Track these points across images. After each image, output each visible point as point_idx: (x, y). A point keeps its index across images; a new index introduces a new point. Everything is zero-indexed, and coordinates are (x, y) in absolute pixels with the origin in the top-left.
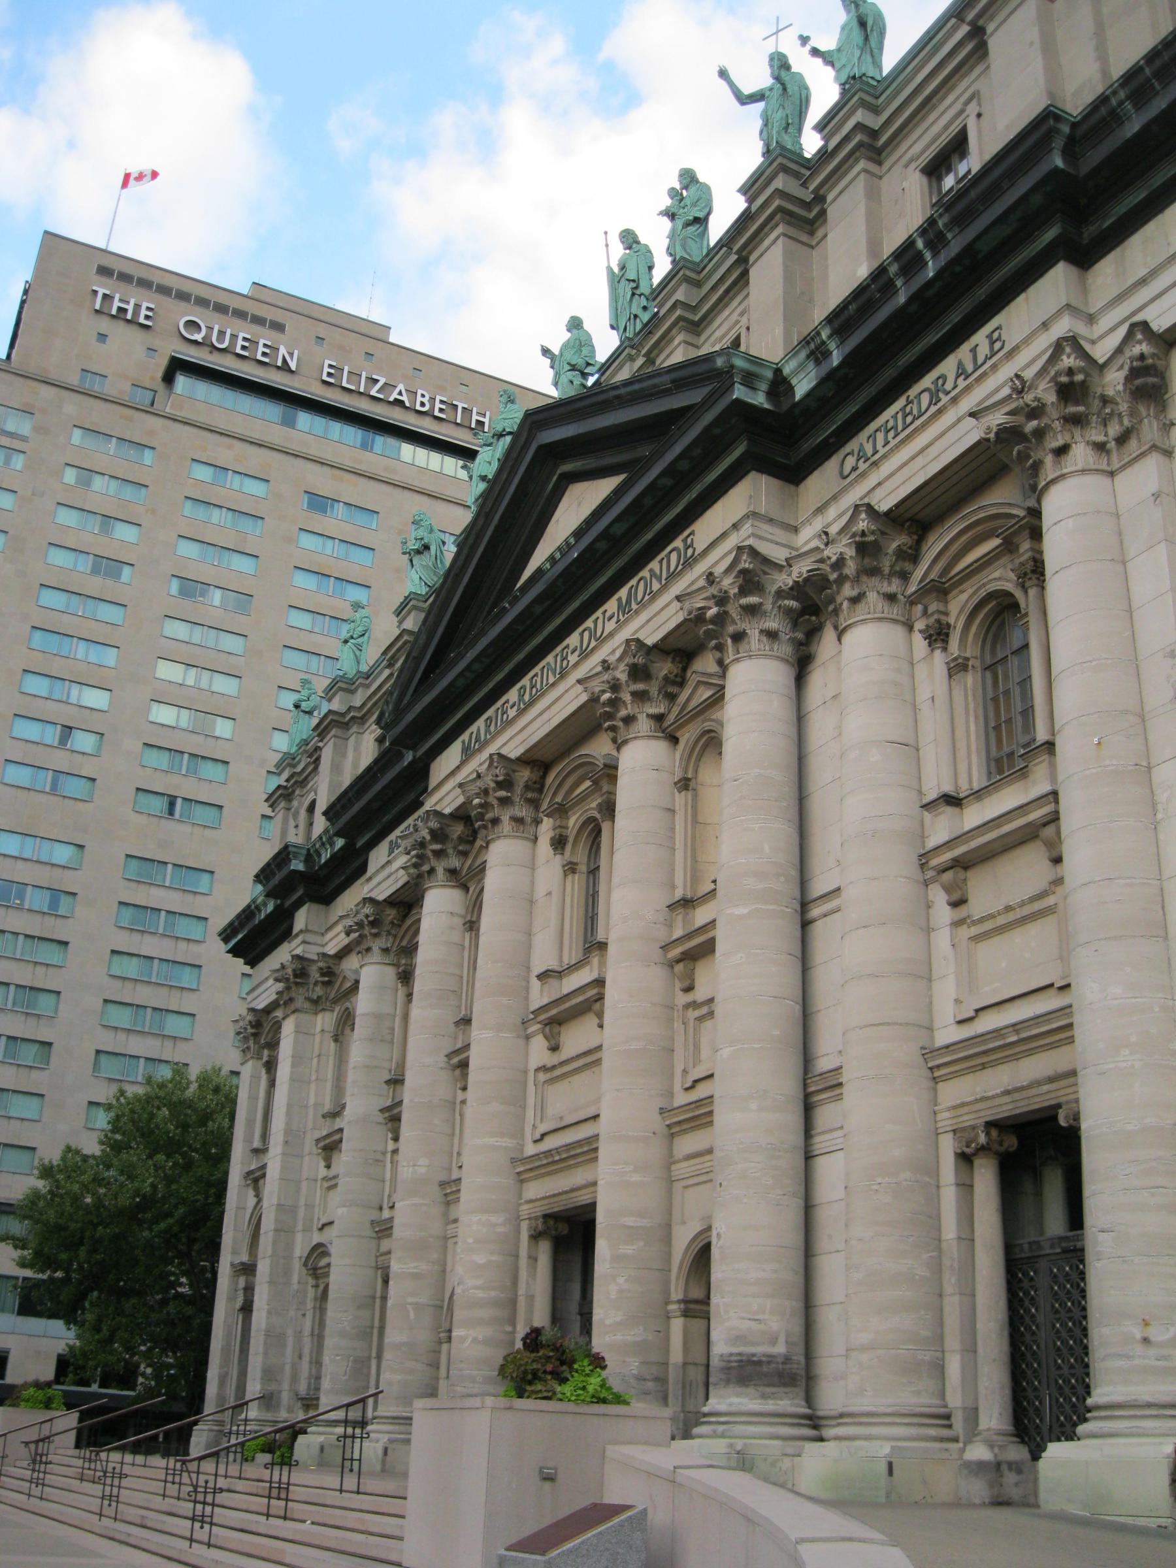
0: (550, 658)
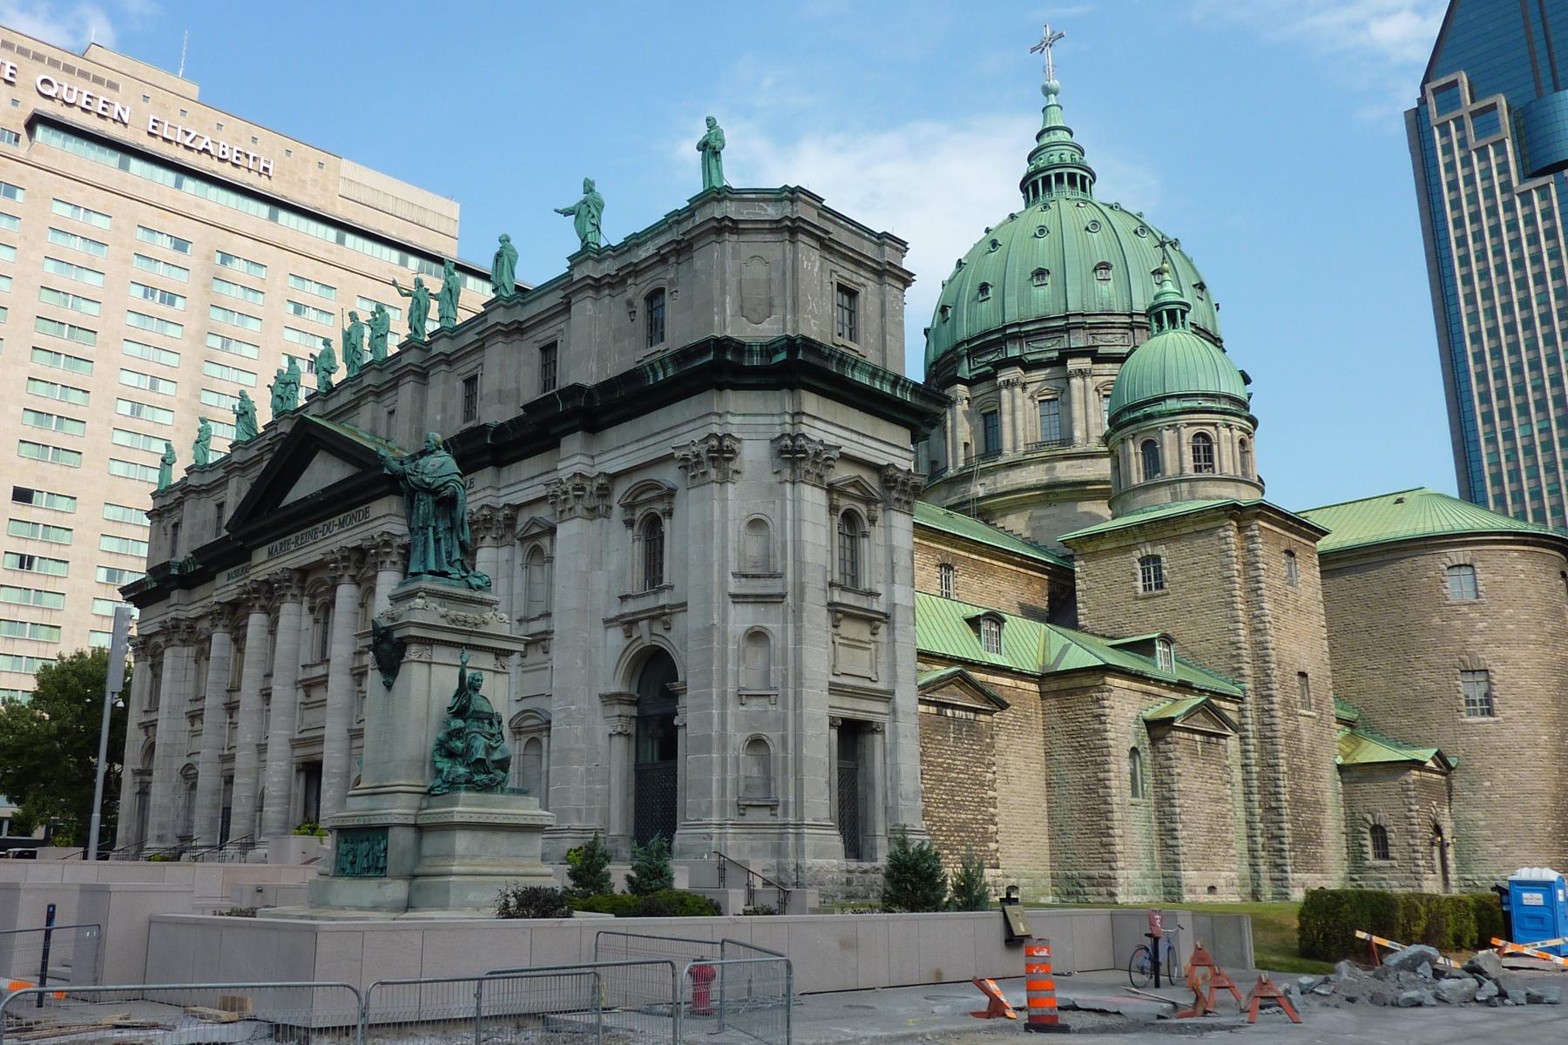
0: (309, 529)
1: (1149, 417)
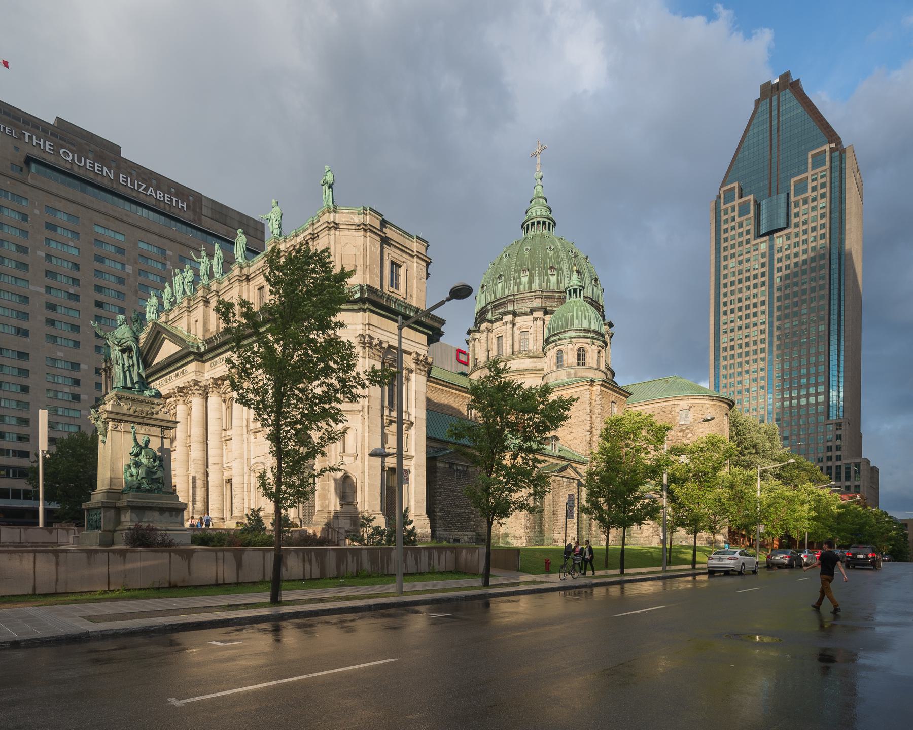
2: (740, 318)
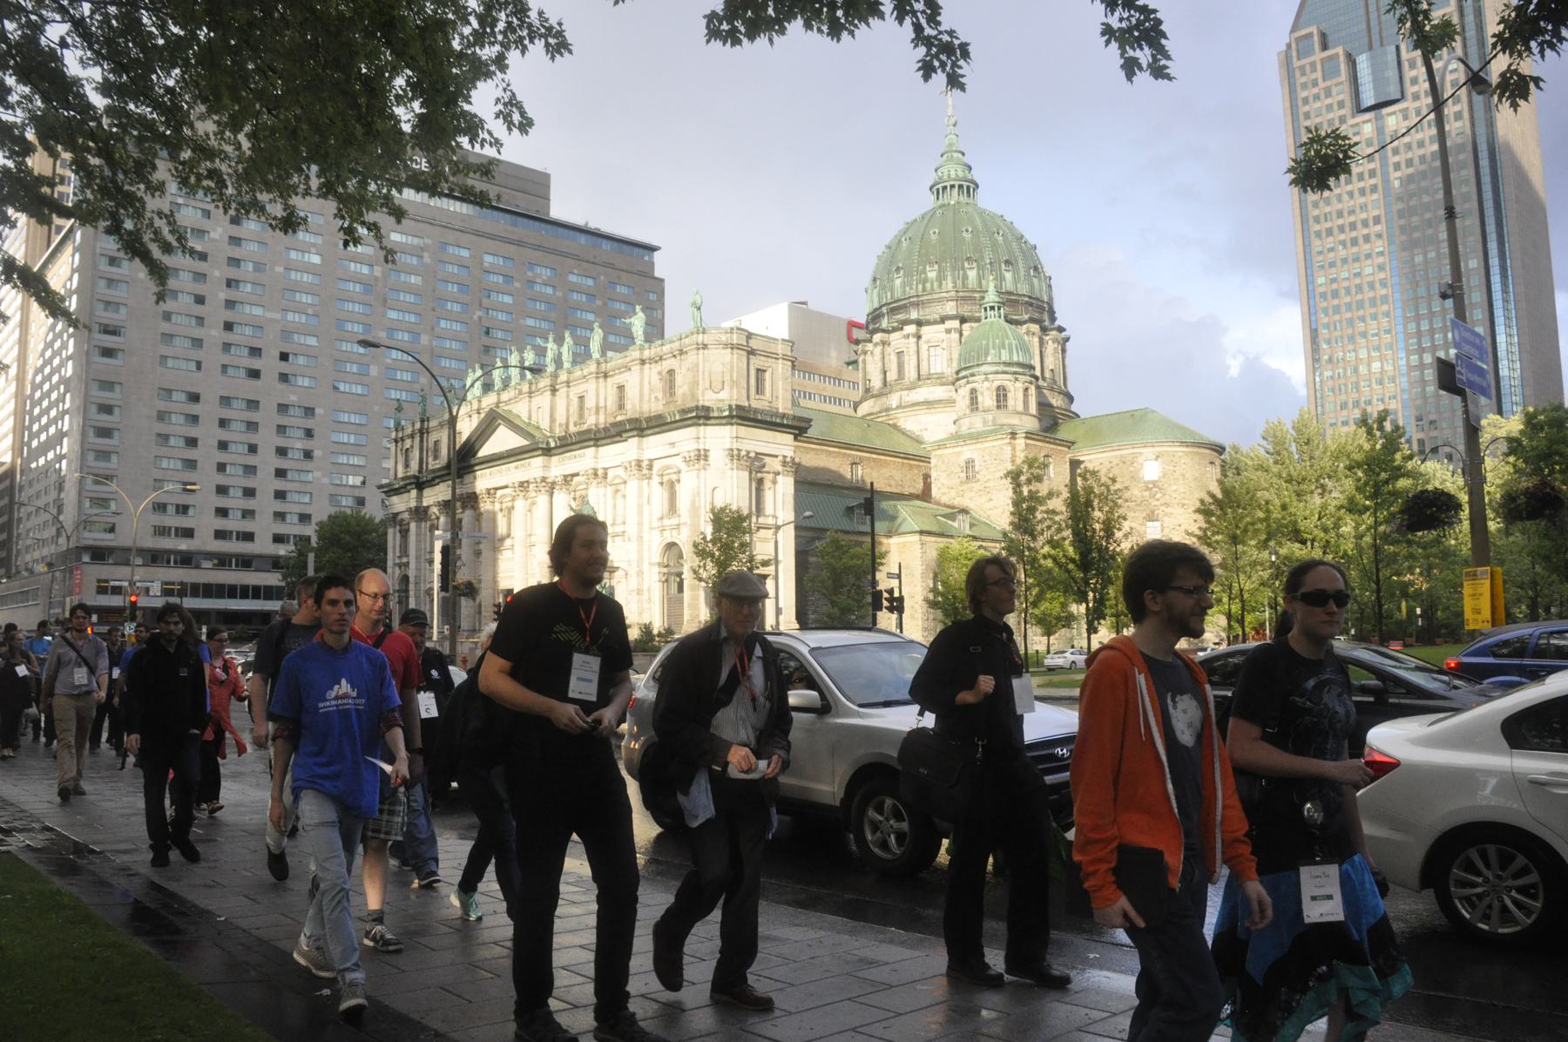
1: (973, 375)
2: (1343, 243)
